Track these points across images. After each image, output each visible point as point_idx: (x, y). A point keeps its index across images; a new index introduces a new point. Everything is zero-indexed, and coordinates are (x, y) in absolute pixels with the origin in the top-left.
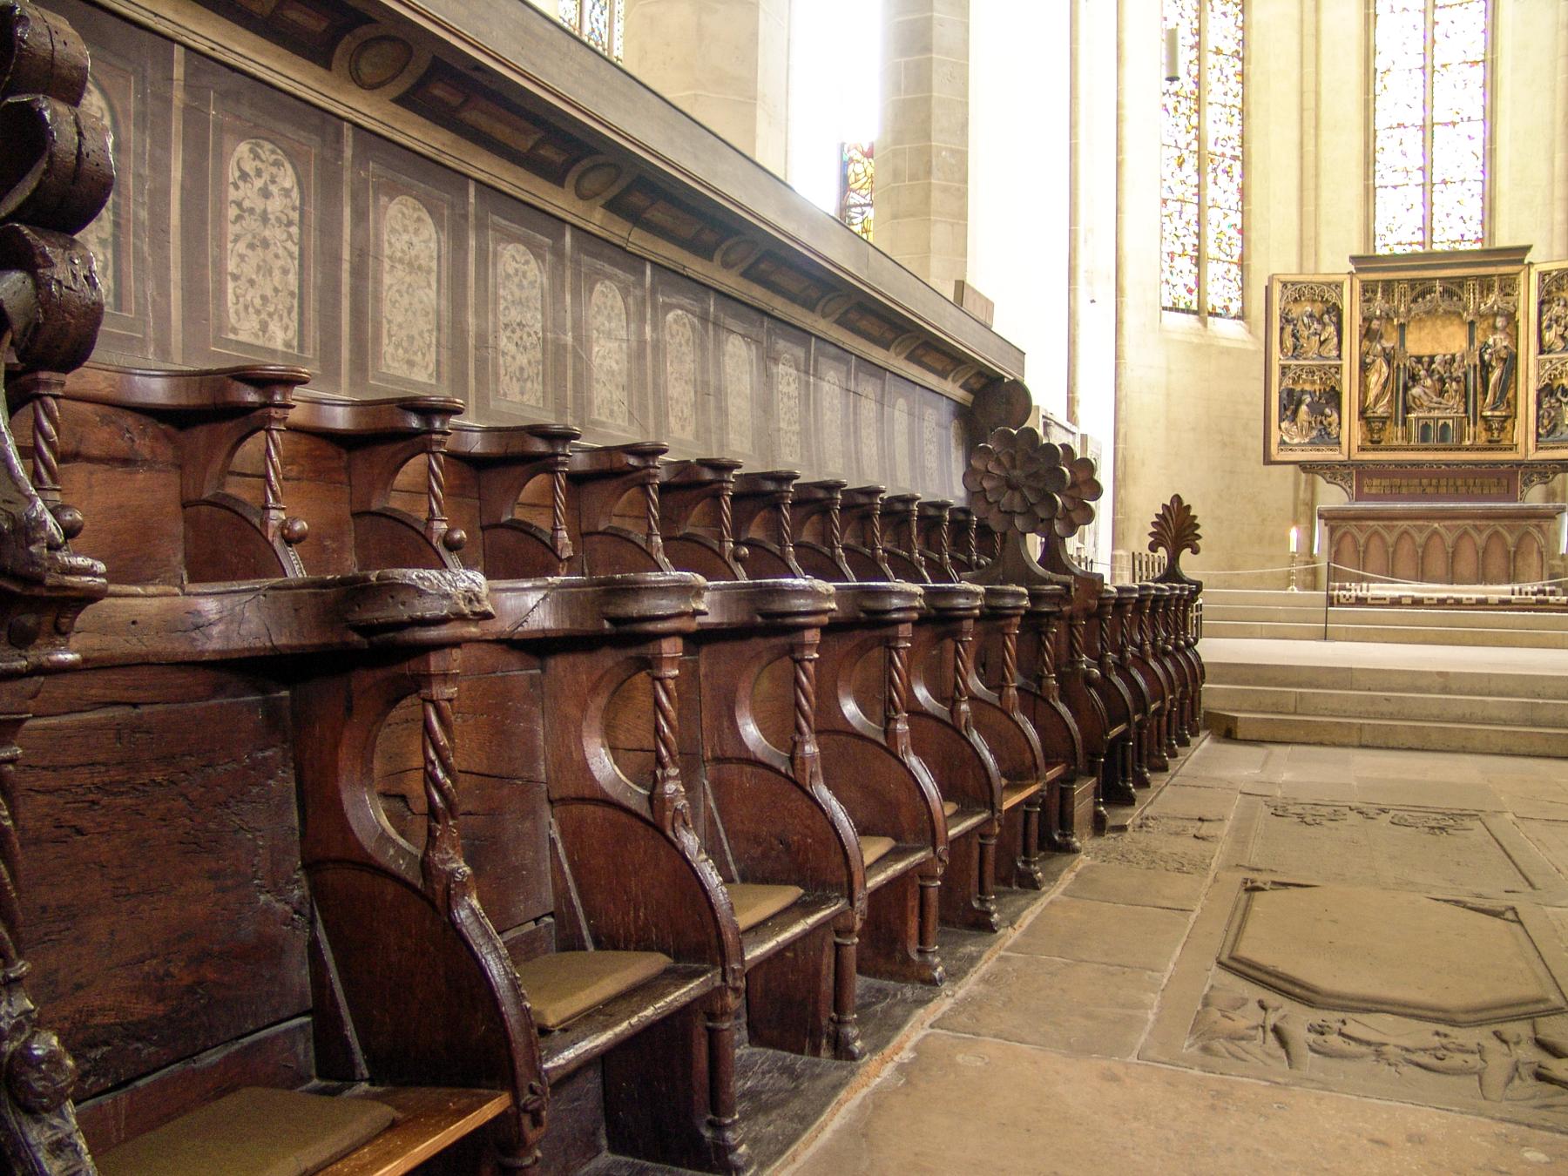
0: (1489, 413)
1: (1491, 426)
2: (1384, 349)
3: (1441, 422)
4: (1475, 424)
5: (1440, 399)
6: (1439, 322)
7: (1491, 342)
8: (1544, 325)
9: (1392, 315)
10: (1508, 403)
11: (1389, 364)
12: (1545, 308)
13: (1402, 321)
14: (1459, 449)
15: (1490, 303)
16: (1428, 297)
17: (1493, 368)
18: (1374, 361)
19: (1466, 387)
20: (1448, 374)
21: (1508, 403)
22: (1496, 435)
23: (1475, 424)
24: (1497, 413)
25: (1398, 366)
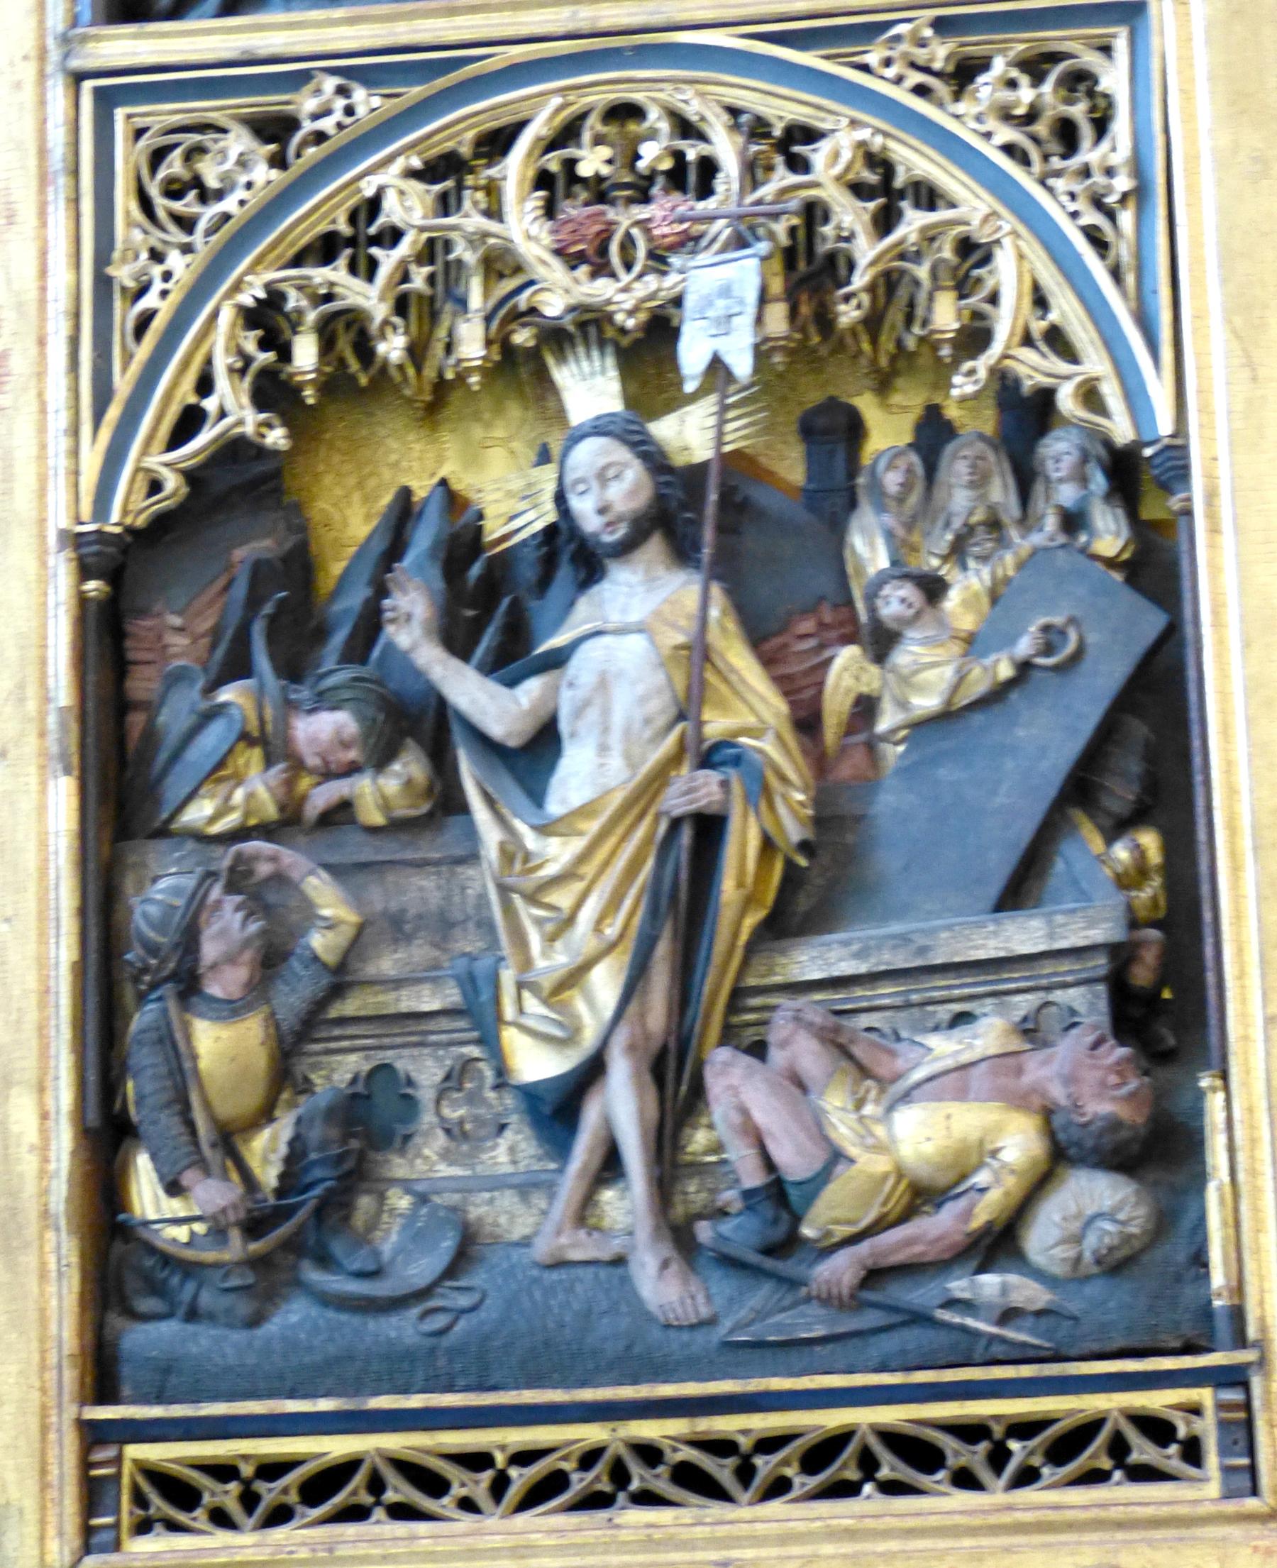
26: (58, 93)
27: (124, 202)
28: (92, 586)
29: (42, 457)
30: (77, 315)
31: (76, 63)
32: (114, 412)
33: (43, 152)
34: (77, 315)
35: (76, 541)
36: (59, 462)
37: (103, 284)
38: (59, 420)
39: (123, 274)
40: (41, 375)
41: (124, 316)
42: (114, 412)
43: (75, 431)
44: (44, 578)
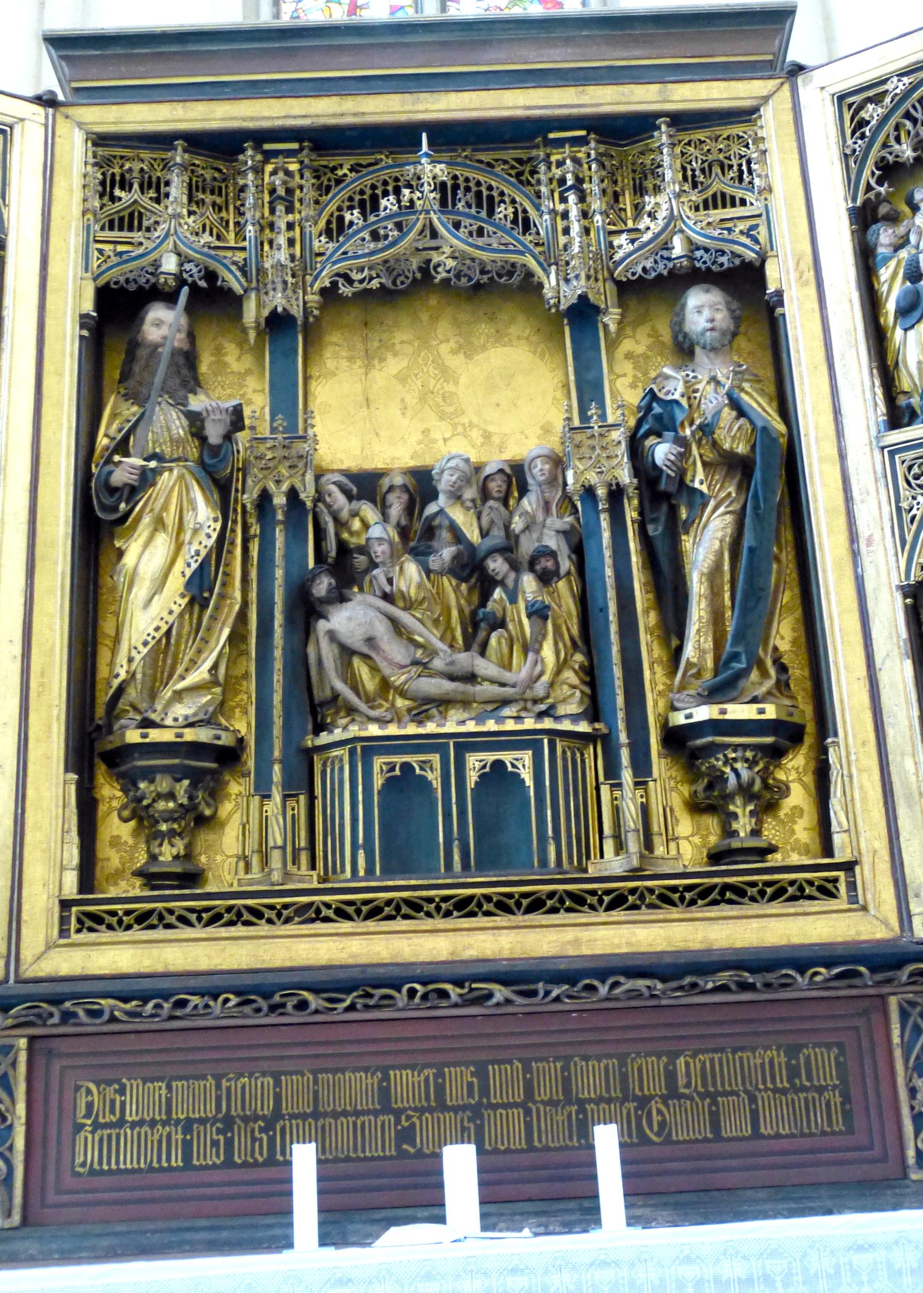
0: (703, 713)
1: (716, 780)
2: (196, 421)
3: (475, 762)
4: (642, 767)
5: (465, 660)
6: (444, 327)
7: (675, 389)
8: (891, 307)
9: (233, 281)
10: (782, 668)
11: (225, 507)
12: (884, 236)
13: (278, 300)
14: (578, 901)
15: (650, 227)
16: (388, 203)
17: (697, 500)
18: (147, 479)
19: (583, 601)
20: (497, 537)
21: (782, 668)
22: (743, 825)
23: (642, 767)
24: (739, 711)
25: (265, 497)
26: (877, 454)
27: (902, 483)
28: (908, 601)
29: (887, 564)
30: (892, 520)
31: (881, 444)
32: (907, 547)
33: (875, 472)
34: (892, 520)
35: (901, 588)
36: (893, 564)
37: (899, 509)
38: (891, 552)
39: (905, 505)
40: (884, 539)
41: (906, 518)
42: (907, 547)
43: (896, 555)
44: (893, 600)
